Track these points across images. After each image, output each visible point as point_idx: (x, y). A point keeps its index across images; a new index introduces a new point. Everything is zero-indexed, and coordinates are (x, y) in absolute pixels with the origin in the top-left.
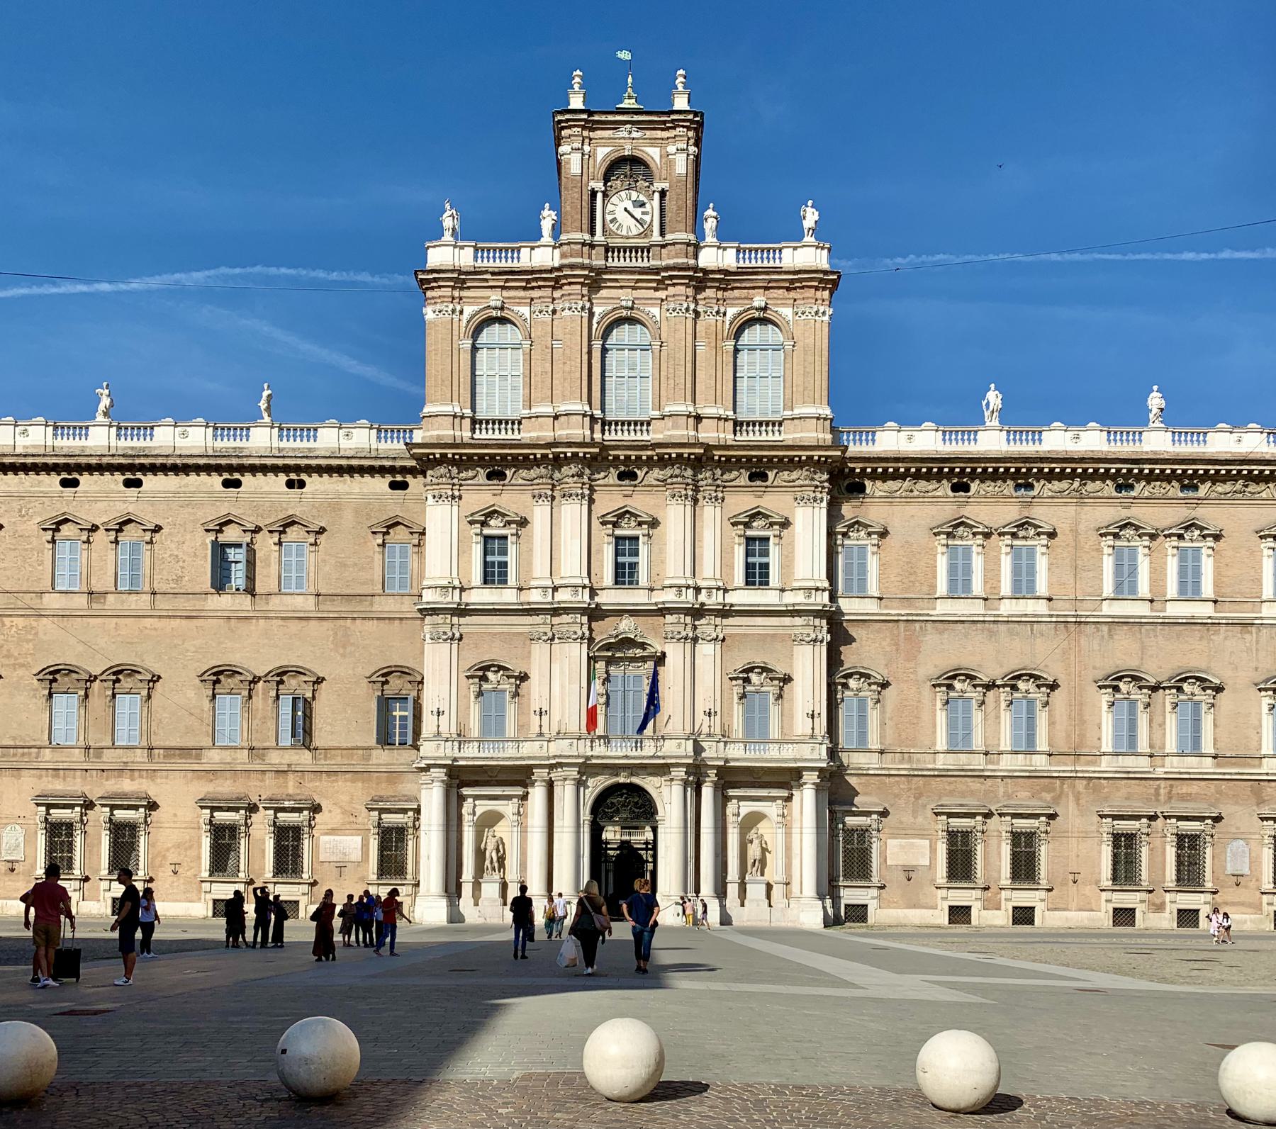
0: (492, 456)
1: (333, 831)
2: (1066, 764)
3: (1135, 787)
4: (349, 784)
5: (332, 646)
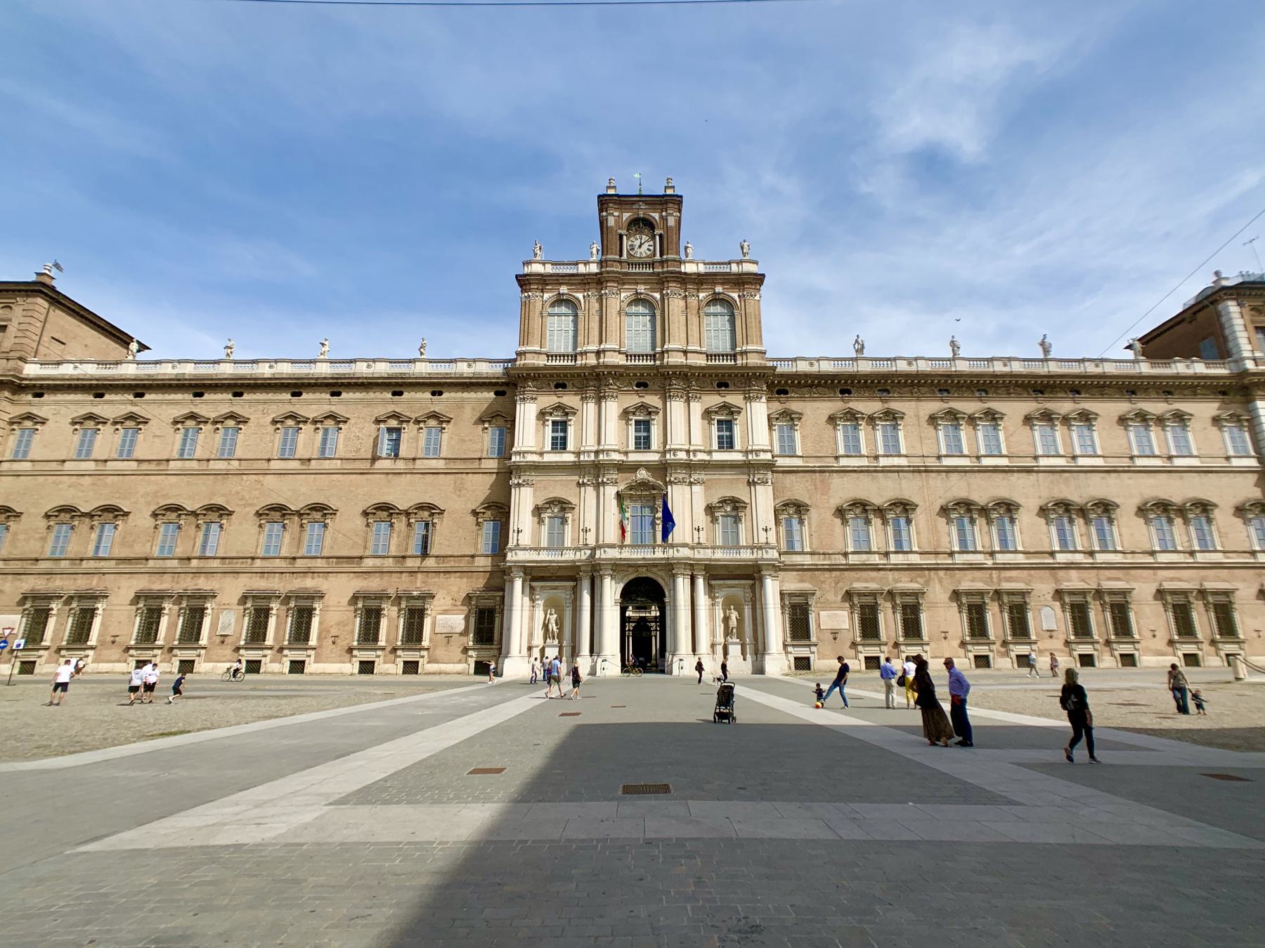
0: (558, 375)
1: (445, 612)
2: (931, 560)
3: (977, 574)
4: (458, 579)
5: (452, 491)
